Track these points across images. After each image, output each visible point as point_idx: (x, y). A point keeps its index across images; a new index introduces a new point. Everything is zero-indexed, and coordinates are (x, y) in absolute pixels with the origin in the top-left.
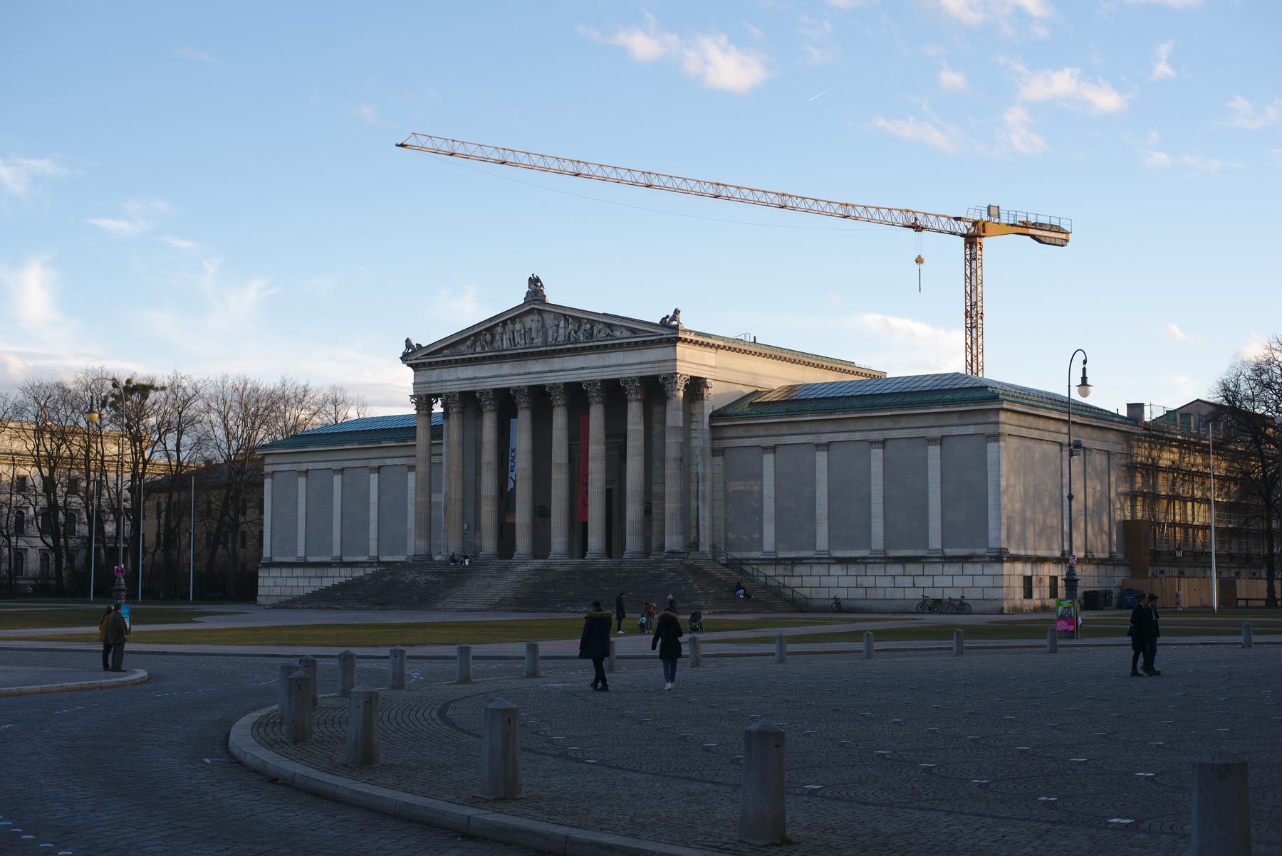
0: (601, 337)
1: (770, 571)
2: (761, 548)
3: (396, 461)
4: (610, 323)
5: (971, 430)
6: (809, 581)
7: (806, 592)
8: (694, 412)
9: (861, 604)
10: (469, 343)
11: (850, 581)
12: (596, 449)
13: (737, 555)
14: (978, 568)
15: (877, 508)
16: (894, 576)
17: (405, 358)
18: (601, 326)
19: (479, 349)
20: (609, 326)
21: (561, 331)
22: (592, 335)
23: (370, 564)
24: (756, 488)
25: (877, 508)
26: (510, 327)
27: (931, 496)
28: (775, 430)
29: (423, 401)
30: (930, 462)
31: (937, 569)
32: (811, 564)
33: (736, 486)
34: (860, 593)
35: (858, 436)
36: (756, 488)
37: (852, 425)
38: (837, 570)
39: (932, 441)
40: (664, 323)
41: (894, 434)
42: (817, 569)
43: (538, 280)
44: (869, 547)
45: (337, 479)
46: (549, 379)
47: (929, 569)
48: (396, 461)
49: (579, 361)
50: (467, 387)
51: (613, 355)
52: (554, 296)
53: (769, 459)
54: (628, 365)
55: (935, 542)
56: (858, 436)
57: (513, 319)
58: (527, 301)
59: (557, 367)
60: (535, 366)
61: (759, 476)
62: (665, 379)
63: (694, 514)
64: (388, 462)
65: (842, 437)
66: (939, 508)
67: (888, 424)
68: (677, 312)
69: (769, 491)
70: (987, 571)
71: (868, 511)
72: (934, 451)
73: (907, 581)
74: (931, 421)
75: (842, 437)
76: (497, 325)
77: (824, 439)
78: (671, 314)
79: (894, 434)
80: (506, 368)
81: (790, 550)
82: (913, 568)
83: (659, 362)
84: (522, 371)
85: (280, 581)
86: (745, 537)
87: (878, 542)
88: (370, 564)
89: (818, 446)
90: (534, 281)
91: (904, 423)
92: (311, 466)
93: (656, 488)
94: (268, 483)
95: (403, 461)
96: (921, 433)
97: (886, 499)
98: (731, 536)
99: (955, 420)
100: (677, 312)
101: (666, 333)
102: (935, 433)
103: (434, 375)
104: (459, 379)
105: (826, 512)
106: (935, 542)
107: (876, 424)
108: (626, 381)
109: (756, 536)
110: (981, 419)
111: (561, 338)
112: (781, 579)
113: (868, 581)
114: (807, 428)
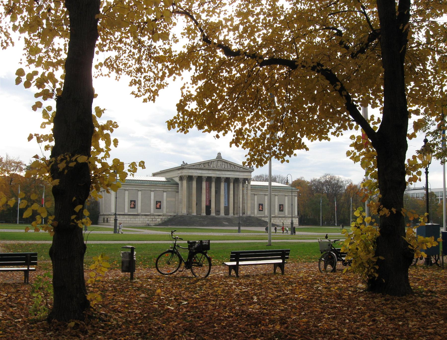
12: (204, 191)
21: (226, 166)
23: (163, 215)
28: (258, 191)
43: (220, 154)
44: (275, 214)
45: (140, 193)
46: (222, 176)
47: (286, 219)
49: (229, 173)
50: (200, 175)
52: (224, 157)
55: (286, 214)
58: (217, 158)
60: (218, 173)
64: (157, 189)
80: (210, 172)
82: (283, 219)
88: (163, 215)
90: (219, 154)
92: (130, 188)
93: (236, 201)
95: (163, 190)
106: (286, 214)
107: (276, 192)
111: (226, 167)
113: (276, 221)
114: (263, 191)
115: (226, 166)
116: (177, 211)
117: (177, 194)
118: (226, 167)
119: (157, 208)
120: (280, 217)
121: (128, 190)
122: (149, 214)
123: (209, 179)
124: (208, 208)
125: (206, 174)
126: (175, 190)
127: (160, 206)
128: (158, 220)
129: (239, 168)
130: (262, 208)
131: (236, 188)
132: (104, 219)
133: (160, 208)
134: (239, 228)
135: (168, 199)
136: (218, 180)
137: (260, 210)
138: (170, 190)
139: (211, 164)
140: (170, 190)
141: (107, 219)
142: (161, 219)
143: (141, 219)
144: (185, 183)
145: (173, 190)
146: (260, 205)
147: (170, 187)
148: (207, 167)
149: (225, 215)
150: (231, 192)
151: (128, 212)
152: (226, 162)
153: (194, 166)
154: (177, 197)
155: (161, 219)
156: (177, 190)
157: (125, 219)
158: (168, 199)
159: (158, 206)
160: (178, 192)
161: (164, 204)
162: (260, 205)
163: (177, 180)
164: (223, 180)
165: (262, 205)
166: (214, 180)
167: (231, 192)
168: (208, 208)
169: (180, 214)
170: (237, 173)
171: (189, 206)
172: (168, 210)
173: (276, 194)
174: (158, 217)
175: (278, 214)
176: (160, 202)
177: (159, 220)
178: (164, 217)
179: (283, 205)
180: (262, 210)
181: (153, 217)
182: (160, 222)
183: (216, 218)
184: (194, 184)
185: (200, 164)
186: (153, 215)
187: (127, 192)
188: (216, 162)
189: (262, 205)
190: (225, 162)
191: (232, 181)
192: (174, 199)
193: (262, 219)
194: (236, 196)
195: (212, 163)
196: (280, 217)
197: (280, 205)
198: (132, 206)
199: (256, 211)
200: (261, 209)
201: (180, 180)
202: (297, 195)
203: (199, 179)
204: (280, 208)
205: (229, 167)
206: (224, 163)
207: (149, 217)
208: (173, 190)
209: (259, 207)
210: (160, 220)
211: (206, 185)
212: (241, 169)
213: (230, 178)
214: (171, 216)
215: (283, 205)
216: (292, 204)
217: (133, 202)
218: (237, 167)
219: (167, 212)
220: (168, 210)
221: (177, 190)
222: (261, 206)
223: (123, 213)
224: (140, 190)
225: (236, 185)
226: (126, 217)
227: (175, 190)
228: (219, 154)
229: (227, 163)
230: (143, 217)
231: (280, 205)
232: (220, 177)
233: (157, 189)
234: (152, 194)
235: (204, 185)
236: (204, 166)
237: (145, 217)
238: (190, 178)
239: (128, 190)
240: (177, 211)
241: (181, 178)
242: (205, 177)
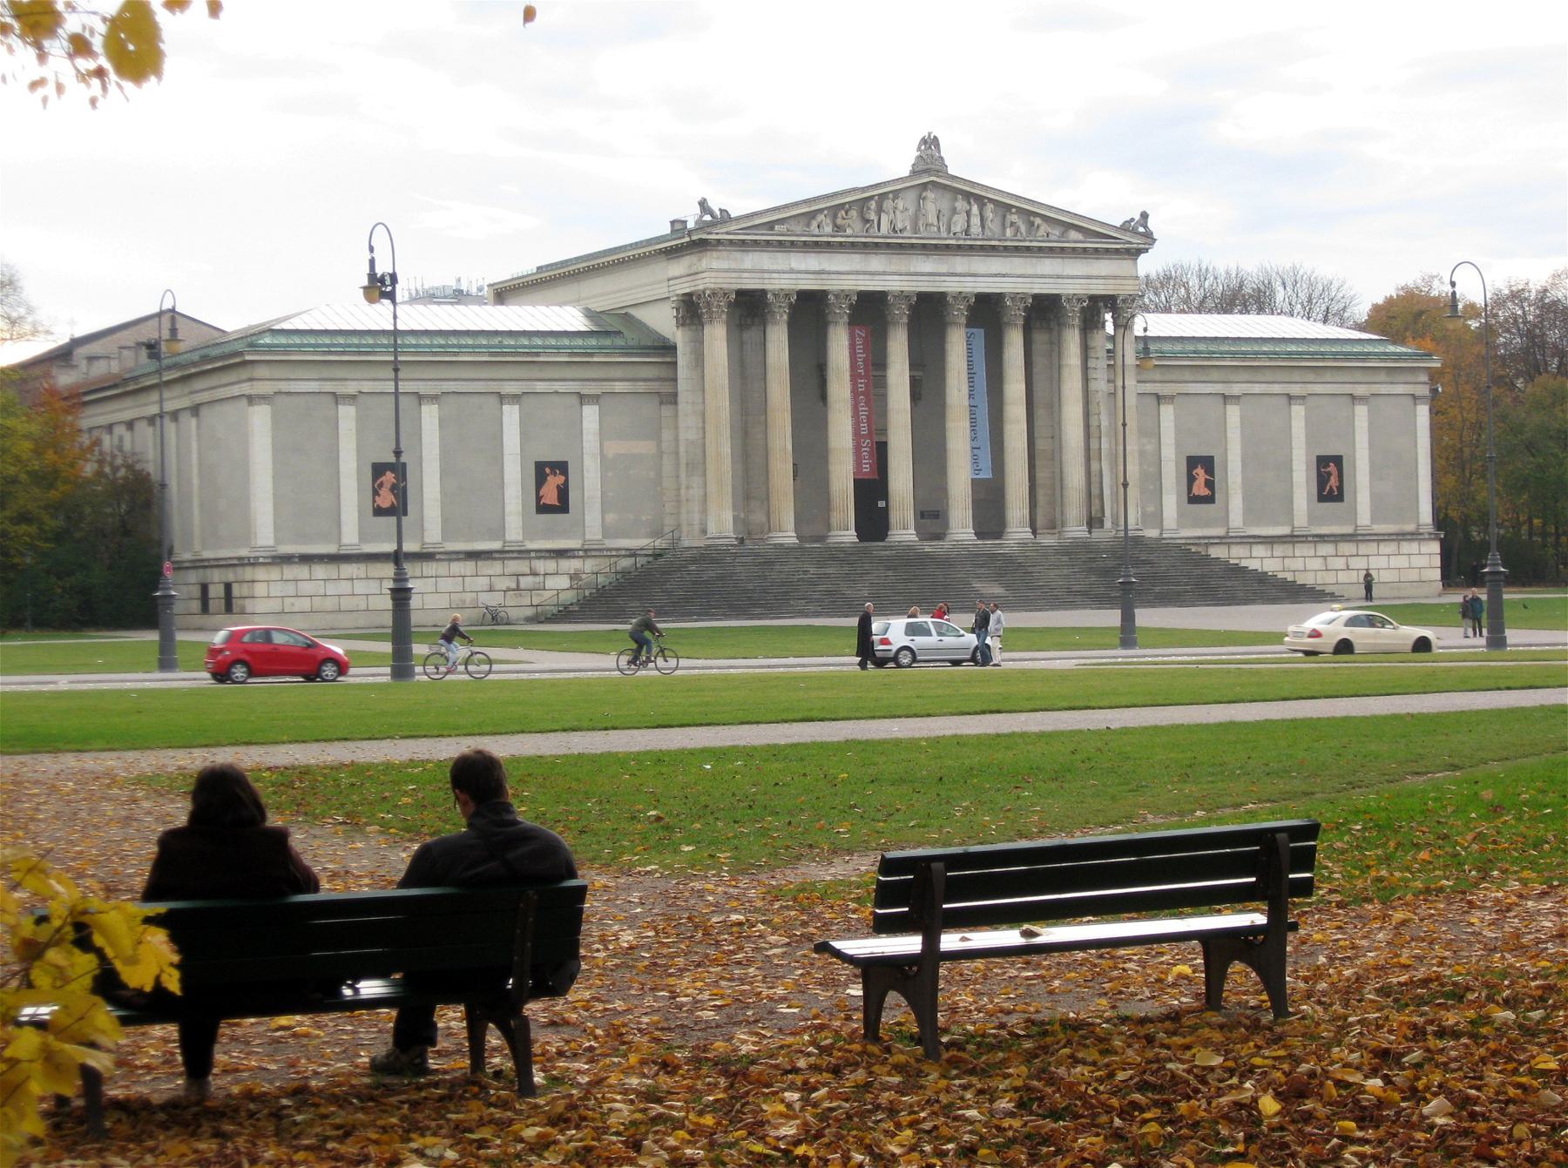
0: (1045, 235)
3: (558, 386)
4: (1066, 224)
5: (1400, 389)
8: (1091, 344)
12: (840, 389)
14: (1413, 547)
16: (1325, 557)
18: (1038, 221)
19: (828, 229)
23: (586, 553)
31: (1371, 548)
35: (1277, 388)
37: (1269, 376)
39: (1362, 399)
40: (1126, 227)
41: (1318, 389)
45: (430, 415)
46: (950, 286)
47: (1363, 549)
48: (558, 386)
51: (1047, 261)
54: (1071, 278)
55: (1364, 518)
56: (1277, 388)
57: (896, 193)
58: (915, 173)
59: (959, 270)
60: (926, 265)
62: (1124, 301)
64: (540, 387)
65: (1257, 388)
66: (1367, 479)
67: (1311, 377)
68: (1145, 216)
74: (1359, 376)
75: (1257, 388)
76: (871, 198)
77: (1236, 389)
78: (1137, 217)
79: (1318, 389)
80: (876, 263)
81: (1196, 525)
83: (1115, 277)
84: (903, 269)
85: (307, 587)
88: (586, 553)
89: (1226, 398)
90: (930, 143)
91: (1328, 377)
93: (1041, 444)
96: (1347, 389)
99: (1382, 377)
100: (1145, 216)
101: (1136, 241)
104: (792, 271)
105: (1239, 479)
107: (1296, 376)
108: (1069, 300)
110: (1410, 378)
111: (976, 228)
114: (1215, 375)
115: (976, 221)
116: (669, 522)
117: (666, 411)
118: (976, 228)
119: (543, 509)
120: (1322, 538)
121: (352, 398)
122: (496, 545)
123: (870, 309)
124: (871, 493)
125: (847, 274)
126: (655, 386)
127: (563, 493)
128: (551, 583)
129: (1056, 232)
130: (1210, 484)
131: (1039, 362)
132: (204, 588)
133: (562, 505)
134: (1128, 618)
135: (615, 448)
136: (929, 312)
137: (1194, 500)
138: (619, 387)
139: (880, 210)
140: (619, 387)
141: (228, 587)
142: (574, 577)
143: (446, 585)
144: (717, 336)
145: (641, 387)
146: (1193, 462)
147: (618, 373)
148: (854, 230)
149: (980, 535)
150: (1015, 388)
151: (363, 537)
152: (975, 196)
153: (770, 225)
154: (667, 435)
155: (574, 577)
156: (665, 388)
157: (345, 587)
158: (615, 448)
159: (550, 496)
160: (672, 398)
161: (589, 483)
162: (1193, 462)
163: (663, 320)
164: (959, 313)
165: (1207, 463)
166: (901, 313)
167: (1015, 388)
168: (871, 493)
169: (691, 540)
170: (1048, 266)
171: (751, 486)
172: (611, 517)
173: (1295, 390)
174: (550, 565)
175: (1312, 519)
176: (561, 467)
177: (558, 584)
178: (589, 565)
179: (1338, 460)
180: (1209, 499)
181: (521, 566)
182: (569, 597)
183: (927, 555)
184: (778, 341)
185: (812, 215)
186: (523, 554)
187: (347, 414)
188: (911, 196)
189: (1207, 463)
190: (968, 196)
191: (1017, 314)
192: (645, 447)
193: (1216, 552)
194: (1040, 413)
195: (888, 204)
196: (1322, 538)
197: (1323, 461)
198: (387, 499)
199: (1171, 502)
200: (1200, 489)
201: (682, 323)
202: (1424, 390)
203: (810, 310)
204: (1322, 480)
205: (994, 226)
206: (961, 204)
207: (495, 567)
208: (641, 387)
209: (1191, 479)
210: (564, 582)
211: (852, 347)
212: (1074, 235)
213: (1000, 297)
214: (632, 553)
215: (1338, 460)
216: (1396, 448)
217: (389, 477)
218: (1044, 228)
219: (607, 532)
220: (611, 517)
221: (665, 388)
222: (1200, 472)
223: (331, 549)
224: (434, 398)
225: (1040, 338)
226: (348, 570)
227: (655, 386)
228: (930, 143)
229: (980, 200)
230: (457, 567)
231: (1323, 461)
232: (943, 295)
233: (540, 387)
234: (511, 415)
235: (840, 347)
236: (838, 228)
237: (468, 567)
238: (749, 308)
239: (352, 398)
240: (669, 522)
241: (691, 309)
242: (842, 295)
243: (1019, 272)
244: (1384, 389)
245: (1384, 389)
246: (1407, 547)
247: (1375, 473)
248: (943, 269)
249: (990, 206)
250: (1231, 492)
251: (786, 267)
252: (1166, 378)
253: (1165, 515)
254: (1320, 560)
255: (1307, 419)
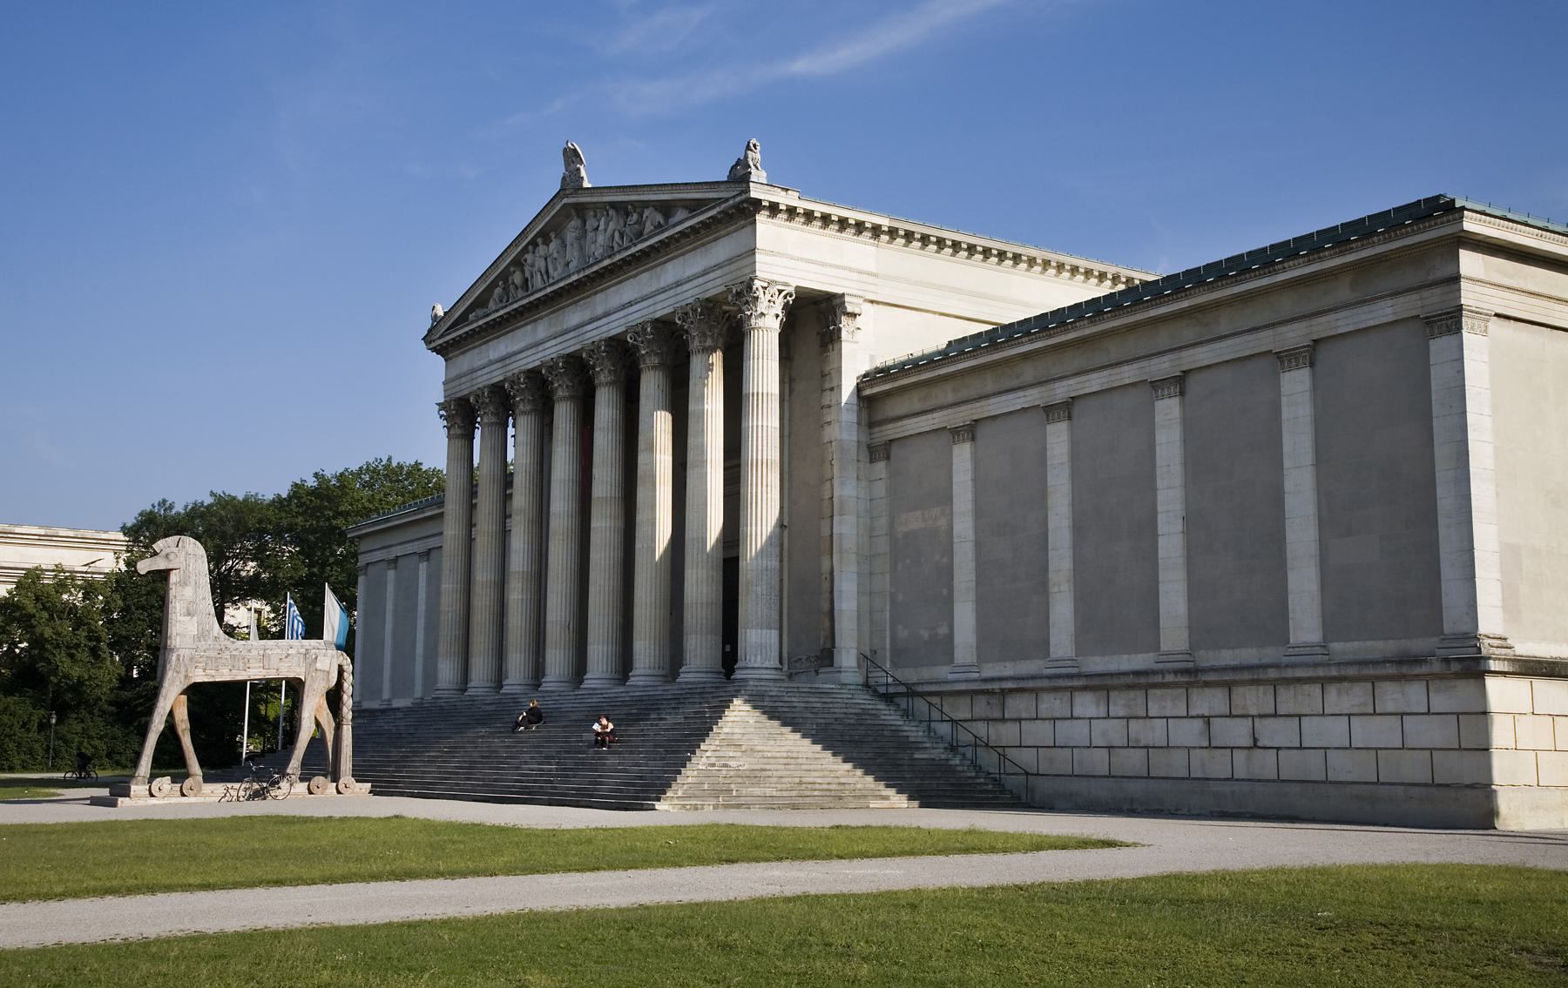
1: (962, 710)
2: (950, 659)
5: (1385, 311)
6: (1039, 732)
7: (1026, 758)
8: (827, 370)
9: (1137, 788)
10: (498, 291)
11: (1114, 732)
13: (910, 675)
14: (1414, 696)
15: (1171, 544)
16: (1207, 719)
17: (427, 339)
20: (666, 208)
22: (640, 234)
24: (943, 522)
25: (1171, 544)
26: (542, 249)
27: (1290, 502)
29: (462, 414)
30: (1286, 413)
32: (1036, 692)
33: (913, 522)
34: (1133, 761)
35: (1128, 374)
36: (943, 522)
38: (1086, 705)
39: (1285, 359)
42: (1052, 704)
47: (1289, 700)
51: (669, 266)
53: (962, 454)
55: (1305, 625)
56: (1128, 374)
57: (544, 236)
59: (599, 311)
61: (945, 498)
63: (826, 586)
65: (1094, 382)
69: (964, 527)
70: (1440, 702)
71: (1150, 557)
72: (1296, 384)
73: (1237, 732)
75: (1094, 382)
76: (525, 250)
77: (1061, 391)
82: (1253, 699)
86: (925, 634)
87: (1174, 633)
94: (361, 579)
97: (1192, 521)
98: (903, 633)
99: (1343, 292)
102: (1295, 335)
103: (470, 359)
104: (491, 363)
106: (1305, 625)
107: (1163, 338)
109: (943, 630)
112: (981, 729)
113: (1153, 732)
114: (1029, 372)
243: (646, 291)
244: (1344, 322)
245: (1344, 322)
246: (1392, 696)
247: (1331, 520)
248: (587, 316)
249: (611, 212)
250: (1053, 589)
251: (485, 361)
252: (965, 393)
253: (956, 641)
254: (1198, 724)
255: (1187, 424)
